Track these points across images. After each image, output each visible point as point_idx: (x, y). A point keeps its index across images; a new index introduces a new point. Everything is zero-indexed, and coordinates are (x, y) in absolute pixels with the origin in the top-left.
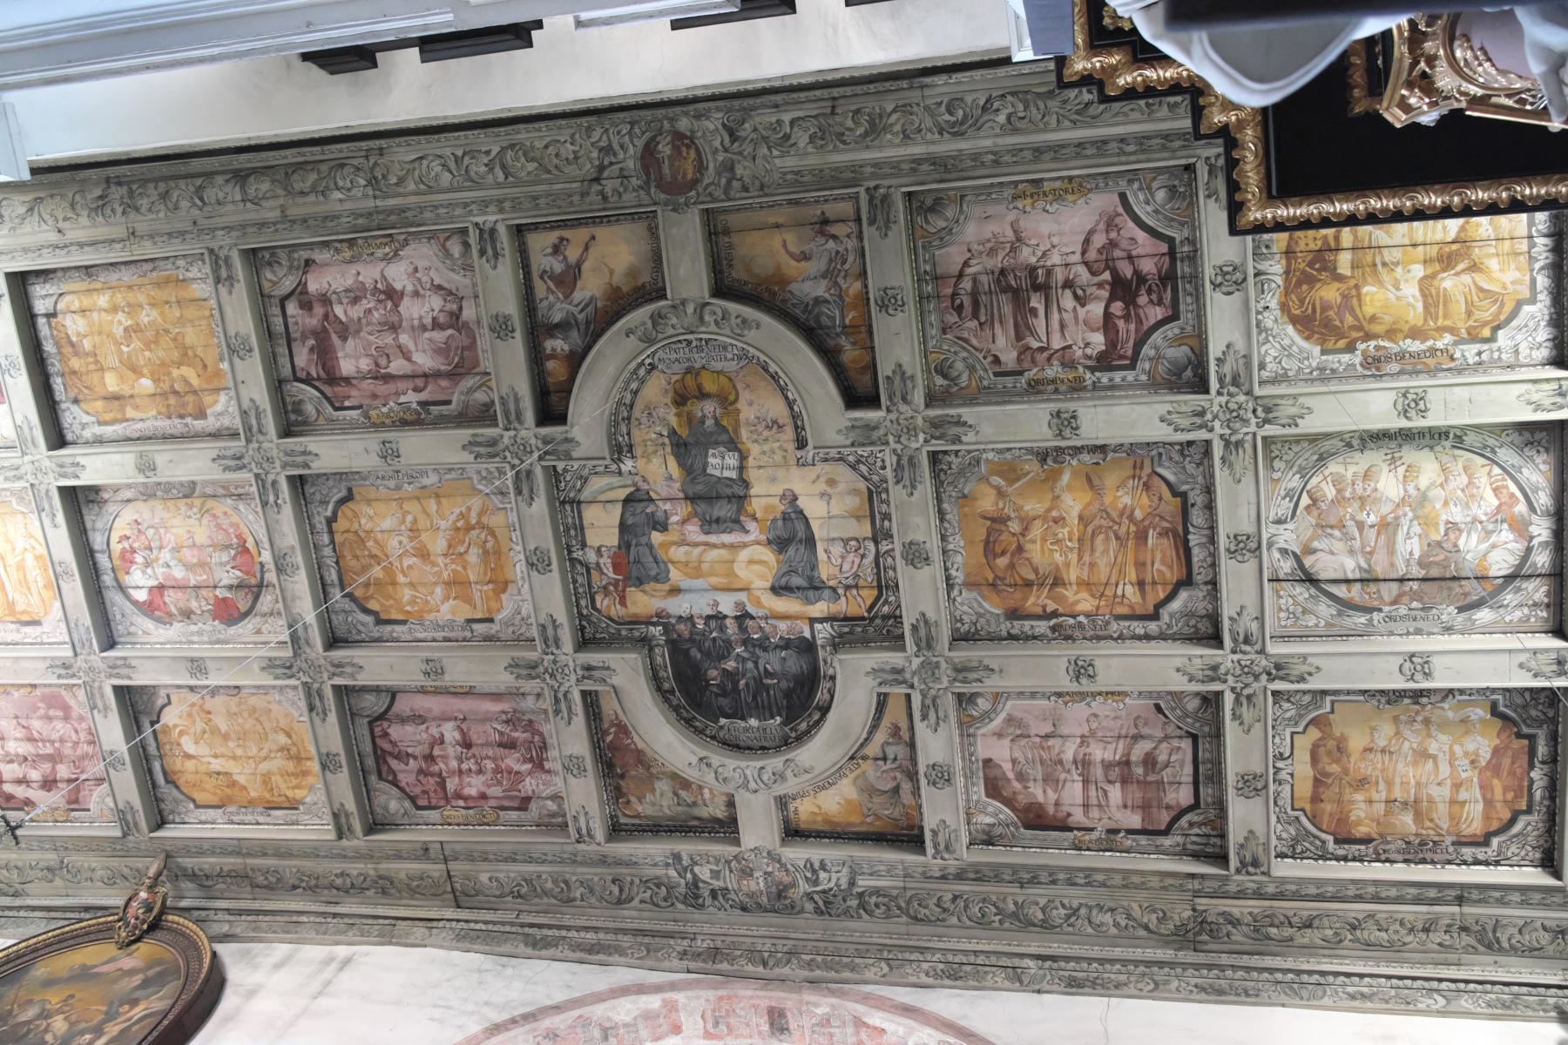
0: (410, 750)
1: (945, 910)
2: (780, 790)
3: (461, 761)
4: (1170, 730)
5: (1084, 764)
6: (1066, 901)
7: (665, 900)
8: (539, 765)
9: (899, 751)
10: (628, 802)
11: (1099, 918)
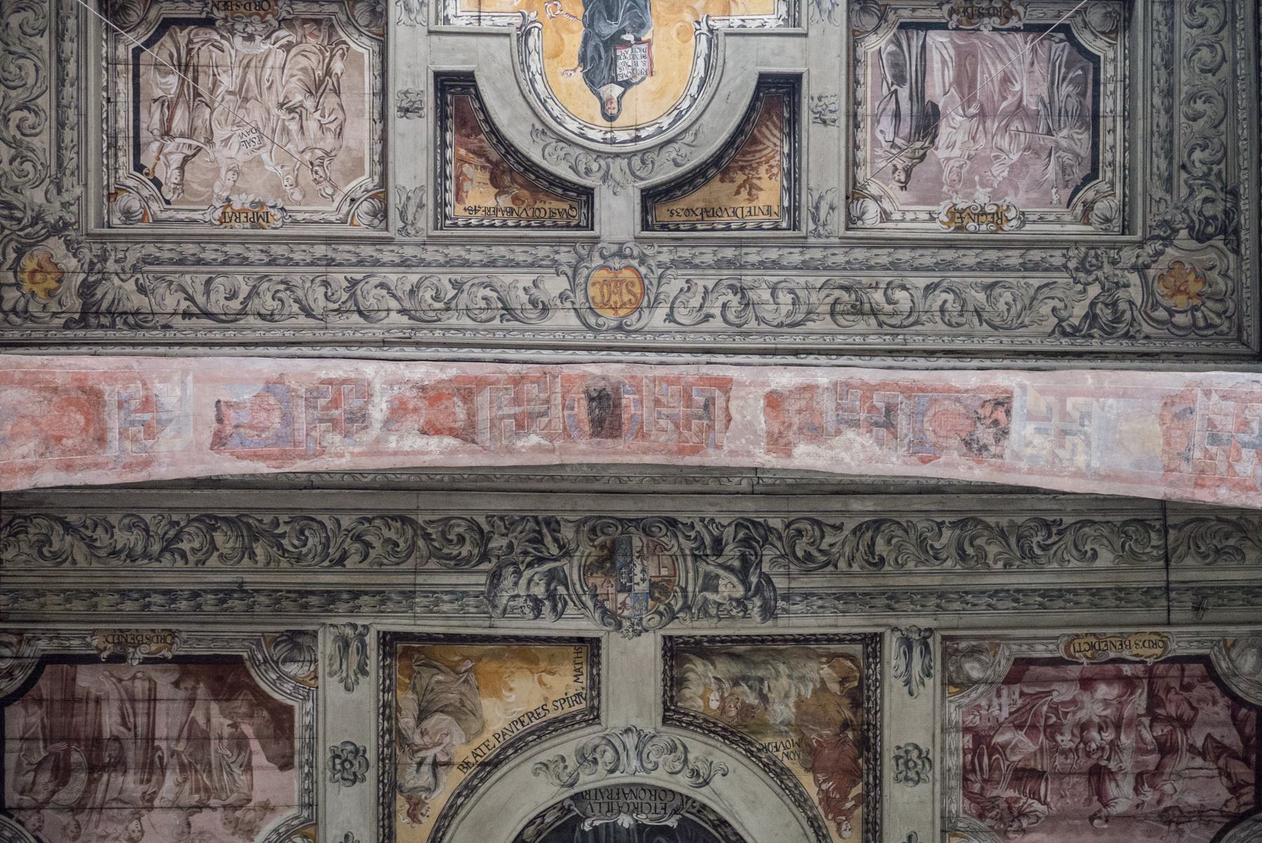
0: (1199, 761)
1: (358, 538)
2: (586, 736)
3: (1114, 746)
4: (33, 820)
5: (152, 767)
6: (180, 563)
7: (800, 533)
8: (981, 741)
9: (413, 778)
10: (843, 681)
11: (133, 539)
